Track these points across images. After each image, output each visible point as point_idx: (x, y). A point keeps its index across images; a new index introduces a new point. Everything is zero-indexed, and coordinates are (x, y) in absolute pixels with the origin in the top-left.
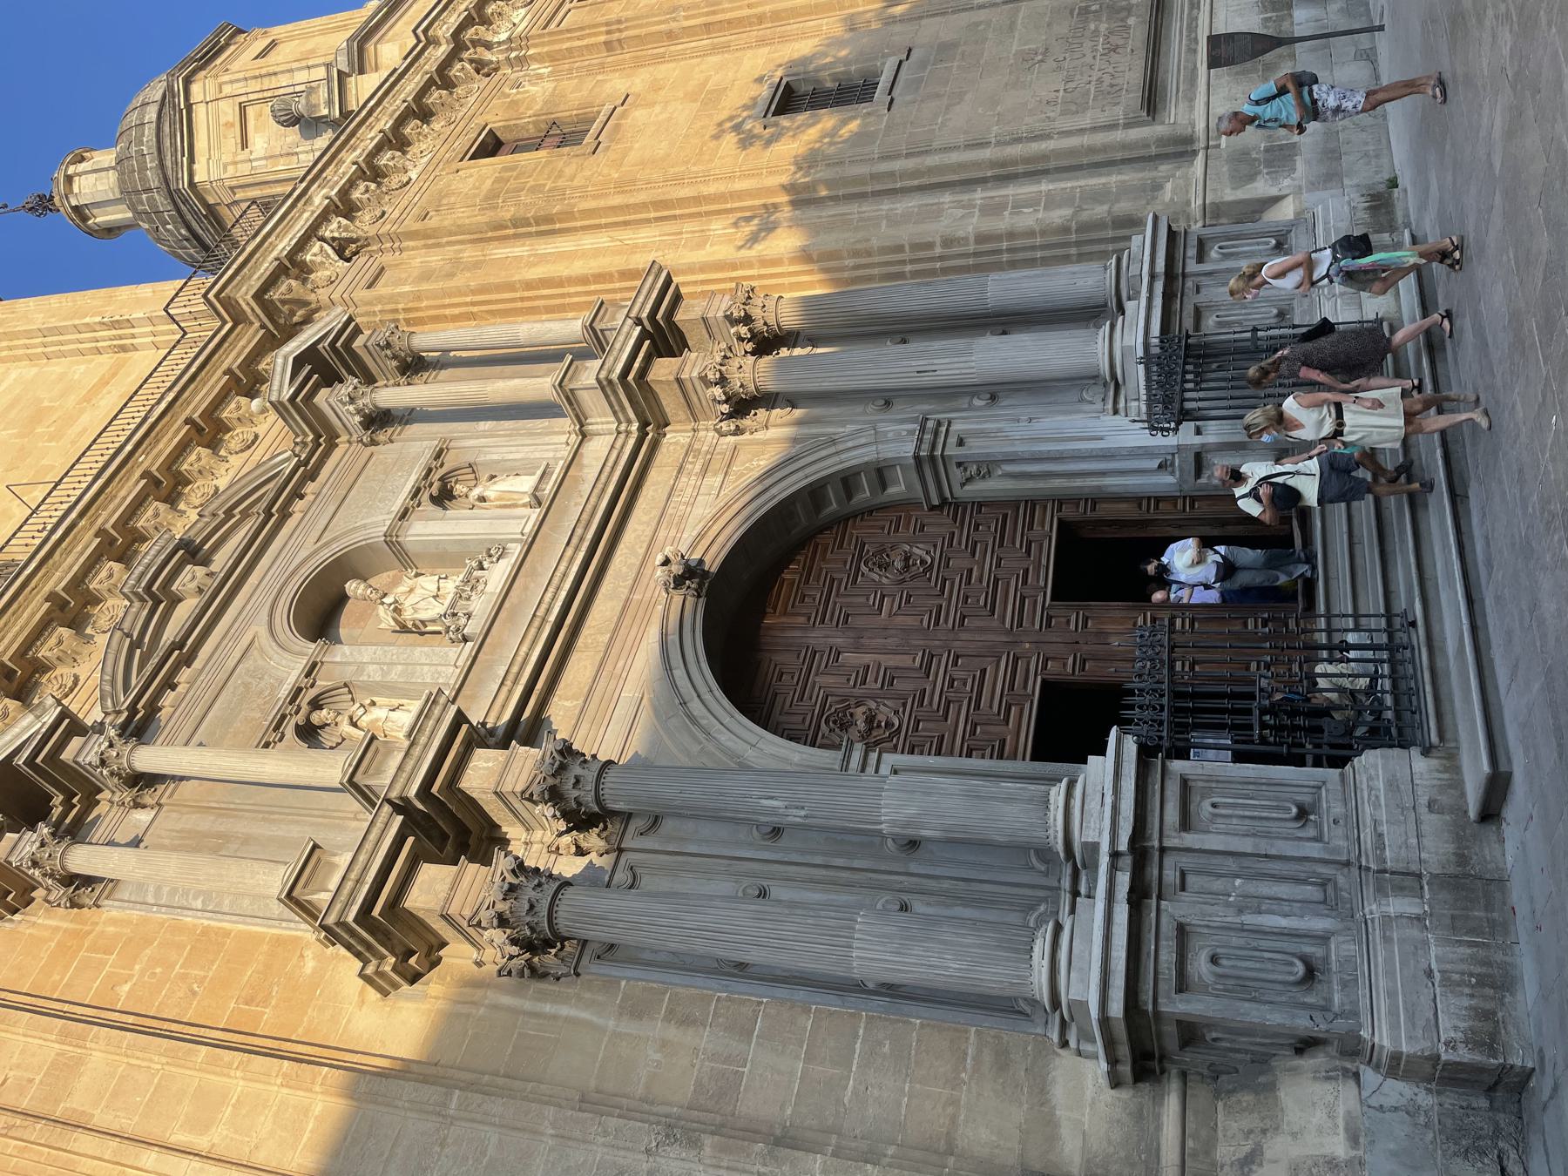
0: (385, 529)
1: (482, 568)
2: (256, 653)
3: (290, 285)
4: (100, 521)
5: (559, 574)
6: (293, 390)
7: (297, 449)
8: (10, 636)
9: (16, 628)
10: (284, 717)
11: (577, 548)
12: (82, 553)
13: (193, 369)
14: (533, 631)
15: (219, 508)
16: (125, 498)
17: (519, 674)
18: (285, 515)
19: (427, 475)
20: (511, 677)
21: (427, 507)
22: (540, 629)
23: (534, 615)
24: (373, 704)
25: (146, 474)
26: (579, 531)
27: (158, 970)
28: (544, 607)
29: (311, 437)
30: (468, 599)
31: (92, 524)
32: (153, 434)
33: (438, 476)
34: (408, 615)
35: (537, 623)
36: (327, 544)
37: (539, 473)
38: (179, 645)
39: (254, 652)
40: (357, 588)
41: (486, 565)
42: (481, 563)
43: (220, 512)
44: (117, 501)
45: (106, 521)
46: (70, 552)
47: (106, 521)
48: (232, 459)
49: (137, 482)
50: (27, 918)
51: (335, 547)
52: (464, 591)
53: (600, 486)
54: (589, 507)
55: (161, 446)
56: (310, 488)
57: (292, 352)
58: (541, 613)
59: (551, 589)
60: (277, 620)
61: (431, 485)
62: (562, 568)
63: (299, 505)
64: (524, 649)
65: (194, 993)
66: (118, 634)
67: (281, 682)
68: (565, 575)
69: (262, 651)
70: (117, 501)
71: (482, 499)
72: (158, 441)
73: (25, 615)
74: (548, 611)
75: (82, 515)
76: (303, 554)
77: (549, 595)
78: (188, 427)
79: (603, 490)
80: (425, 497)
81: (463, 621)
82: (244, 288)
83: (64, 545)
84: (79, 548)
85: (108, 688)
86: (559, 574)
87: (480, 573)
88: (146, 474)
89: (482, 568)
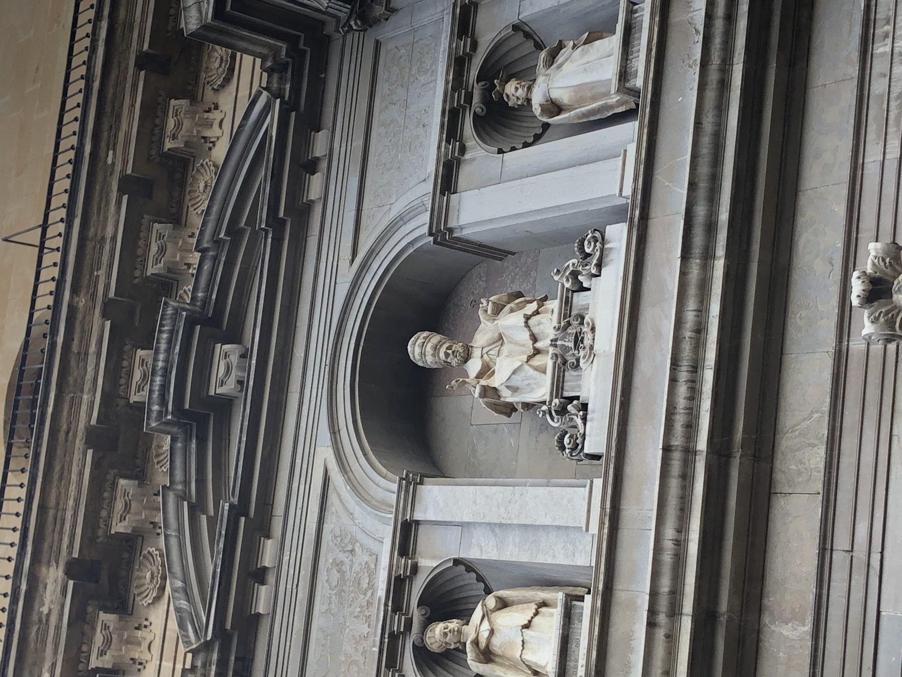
0: (426, 217)
5: (687, 333)
7: (276, 77)
8: (69, 514)
9: (71, 503)
10: (394, 637)
11: (708, 256)
12: (99, 354)
14: (674, 484)
15: (217, 230)
16: (114, 238)
17: (676, 593)
20: (663, 603)
22: (687, 477)
23: (667, 449)
24: (503, 604)
25: (126, 184)
26: (701, 211)
28: (680, 420)
29: (284, 47)
30: (576, 366)
31: (93, 296)
32: (108, 109)
33: (474, 73)
34: (508, 397)
35: (676, 467)
37: (620, 27)
38: (238, 511)
39: (332, 498)
40: (423, 354)
42: (575, 274)
43: (222, 236)
44: (107, 247)
45: (107, 287)
46: (86, 354)
47: (107, 287)
49: (119, 203)
51: (378, 267)
52: (566, 349)
53: (714, 76)
54: (706, 140)
55: (124, 126)
56: (320, 145)
58: (677, 441)
59: (684, 375)
61: (469, 98)
62: (690, 317)
63: (315, 186)
64: (670, 533)
68: (700, 330)
71: (554, 107)
72: (119, 117)
74: (691, 427)
75: (75, 291)
77: (682, 390)
78: (143, 73)
79: (724, 85)
83: (75, 348)
85: (184, 604)
86: (687, 333)
87: (579, 299)
88: (126, 184)
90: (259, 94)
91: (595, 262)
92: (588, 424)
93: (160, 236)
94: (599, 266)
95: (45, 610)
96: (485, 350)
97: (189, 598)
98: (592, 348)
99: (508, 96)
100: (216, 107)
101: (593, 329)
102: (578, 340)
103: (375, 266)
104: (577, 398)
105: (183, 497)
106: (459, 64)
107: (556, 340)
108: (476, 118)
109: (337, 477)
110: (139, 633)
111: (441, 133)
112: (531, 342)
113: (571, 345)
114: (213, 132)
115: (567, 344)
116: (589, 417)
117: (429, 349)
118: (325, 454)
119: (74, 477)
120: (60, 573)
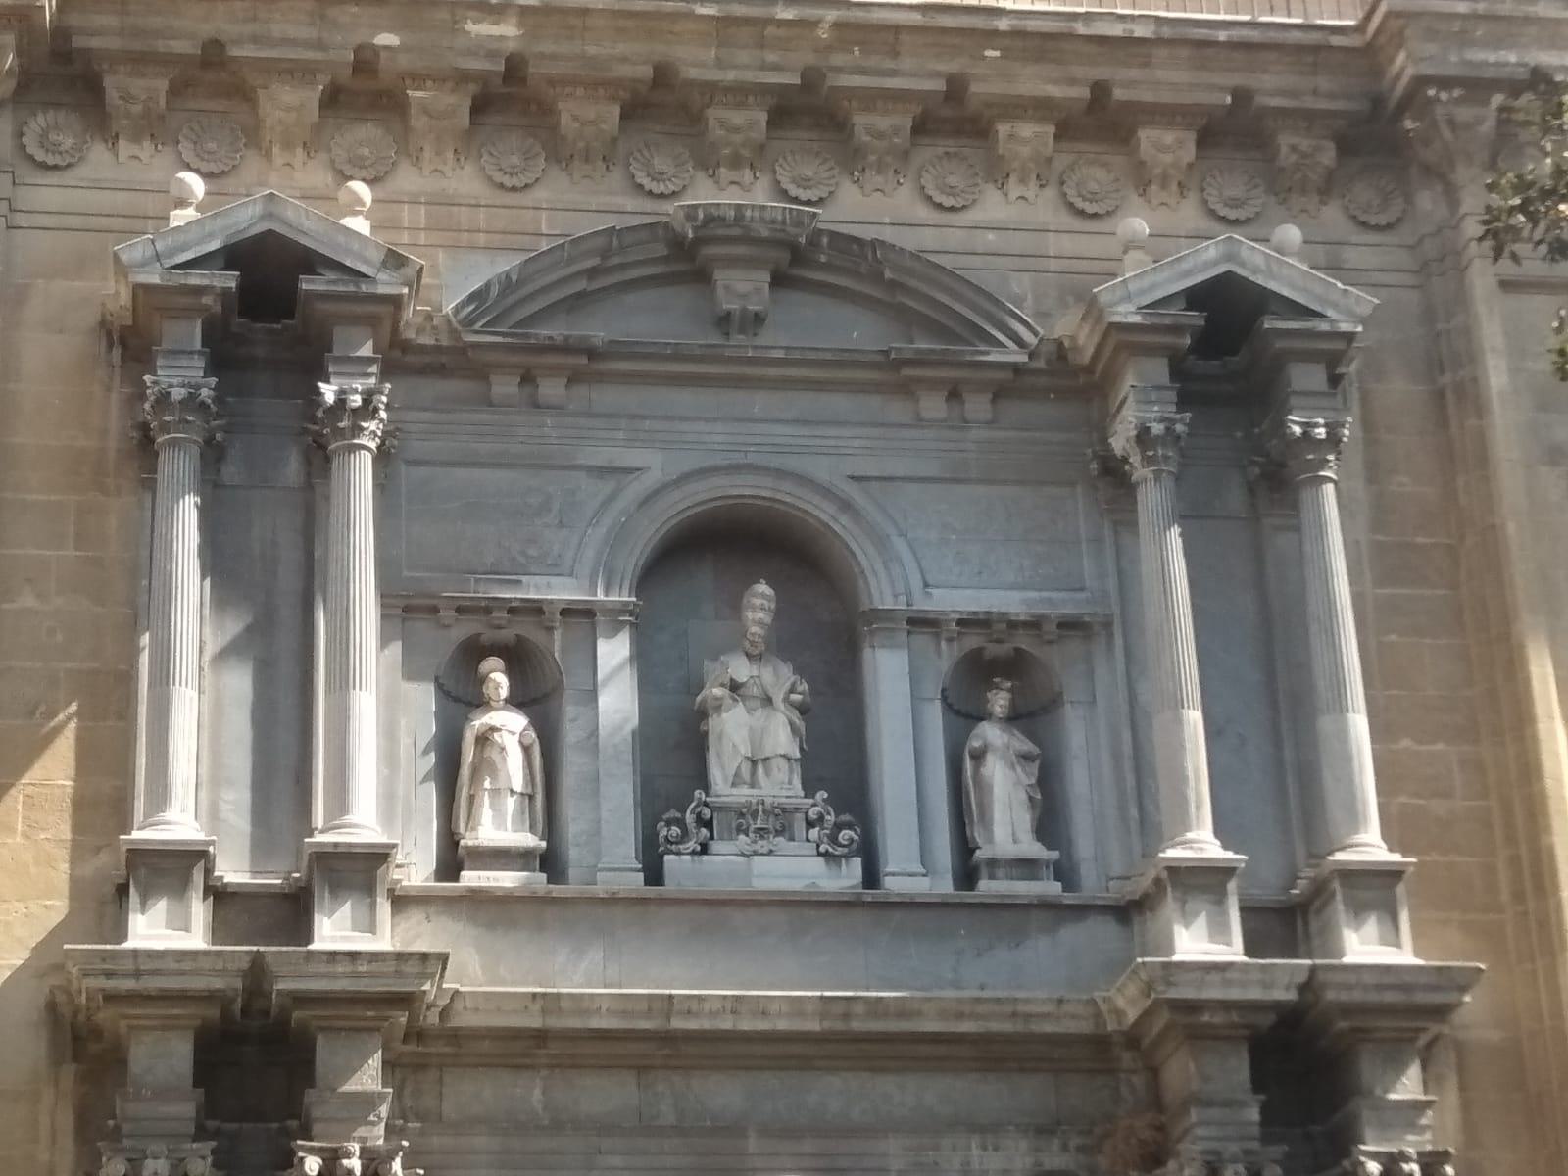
1: (810, 824)
2: (607, 487)
3: (1479, 121)
4: (838, 59)
6: (1137, 319)
12: (764, 67)
13: (1222, 36)
18: (906, 389)
19: (1026, 625)
21: (944, 659)
27: (59, 637)
30: (740, 830)
36: (846, 506)
38: (592, 353)
41: (814, 833)
44: (889, 64)
45: (839, 70)
47: (839, 70)
48: (1050, 193)
49: (937, 75)
50: (117, 370)
51: (842, 525)
57: (1242, 264)
60: (677, 495)
61: (999, 641)
65: (32, 713)
66: (600, 242)
67: (554, 569)
69: (612, 497)
70: (889, 64)
71: (979, 757)
73: (622, 48)
76: (821, 469)
80: (973, 641)
81: (692, 845)
82: (1431, 49)
84: (772, 57)
85: (495, 291)
89: (810, 824)
90: (1036, 334)
91: (831, 850)
92: (688, 857)
93: (896, 131)
94: (826, 854)
95: (470, 27)
96: (757, 680)
97: (502, 294)
98: (755, 853)
99: (996, 694)
100: (1041, 186)
101: (771, 853)
102: (762, 832)
103: (844, 519)
104: (712, 838)
105: (605, 254)
106: (1034, 624)
107: (763, 804)
108: (979, 651)
109: (636, 488)
110: (450, 155)
111: (969, 613)
112: (763, 757)
113: (758, 826)
114: (1014, 189)
115: (759, 818)
116: (696, 858)
117: (760, 615)
118: (655, 464)
119: (622, 48)
120: (511, 46)
